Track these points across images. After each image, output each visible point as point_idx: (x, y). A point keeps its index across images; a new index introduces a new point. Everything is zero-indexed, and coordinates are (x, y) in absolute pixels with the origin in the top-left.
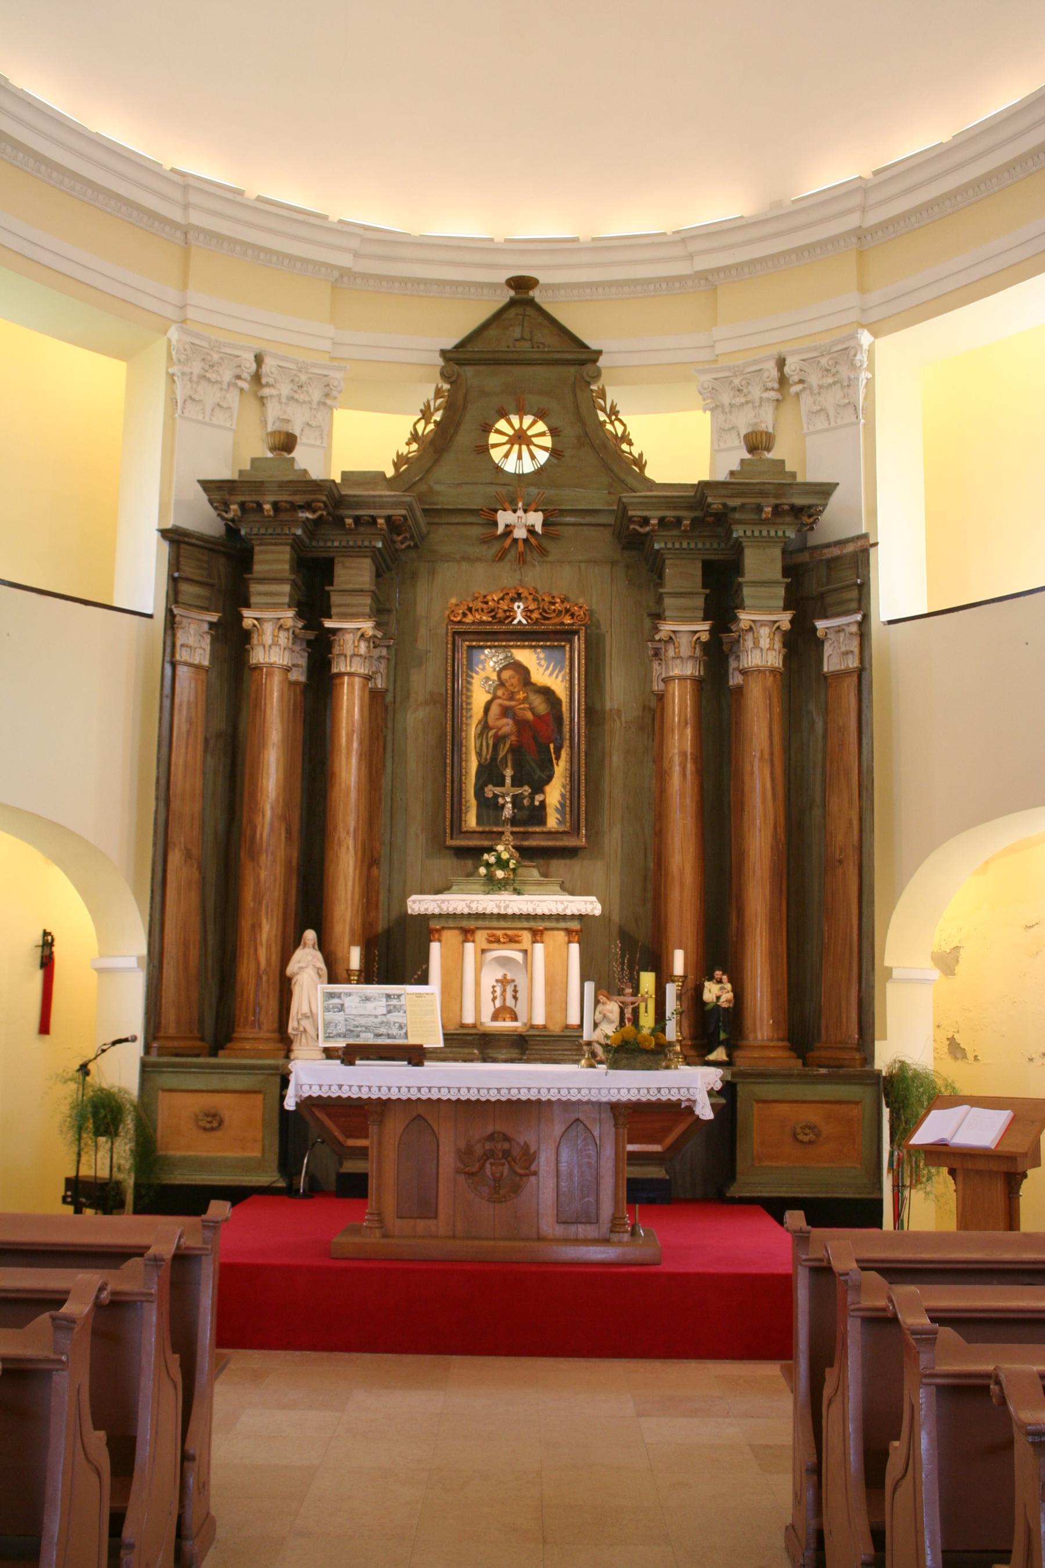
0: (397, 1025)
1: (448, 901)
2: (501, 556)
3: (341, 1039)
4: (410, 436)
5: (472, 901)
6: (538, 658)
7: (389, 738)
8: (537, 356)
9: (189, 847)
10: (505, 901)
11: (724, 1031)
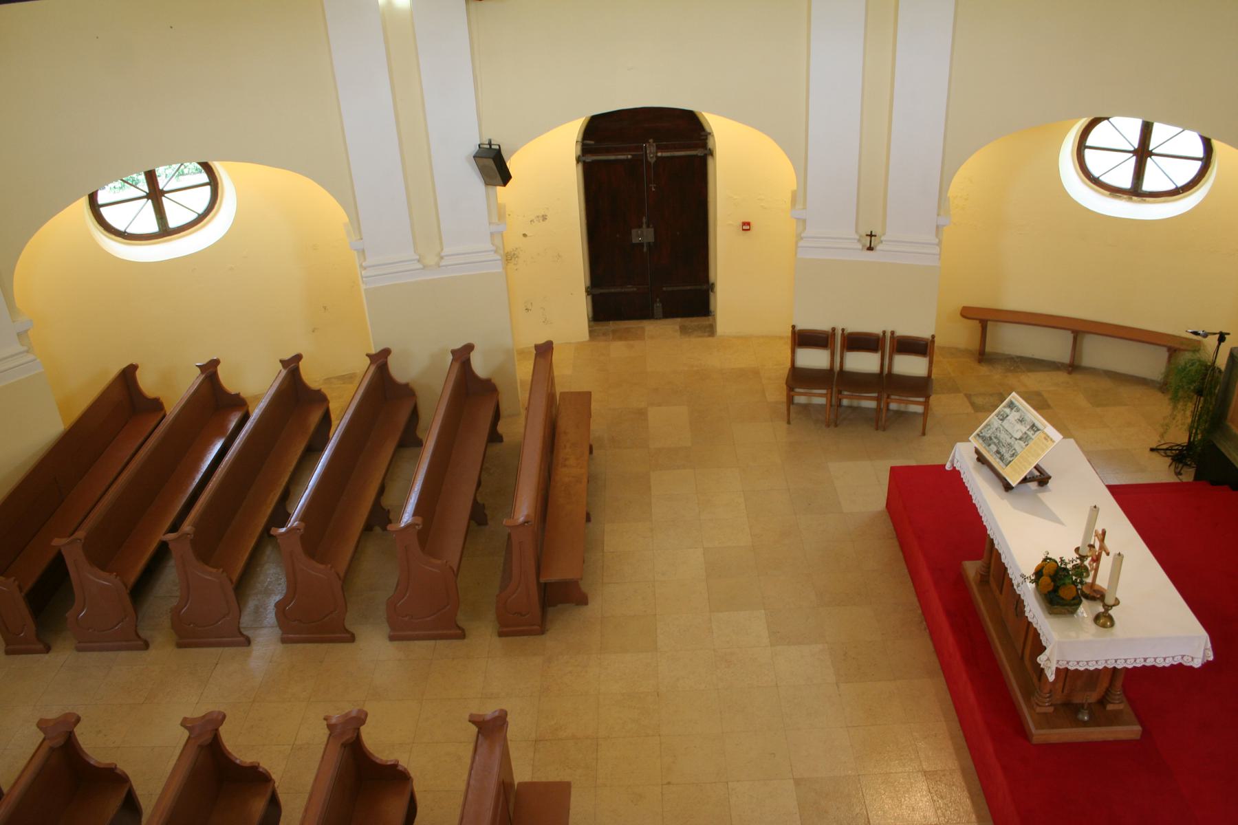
0: (1014, 451)
3: (981, 441)
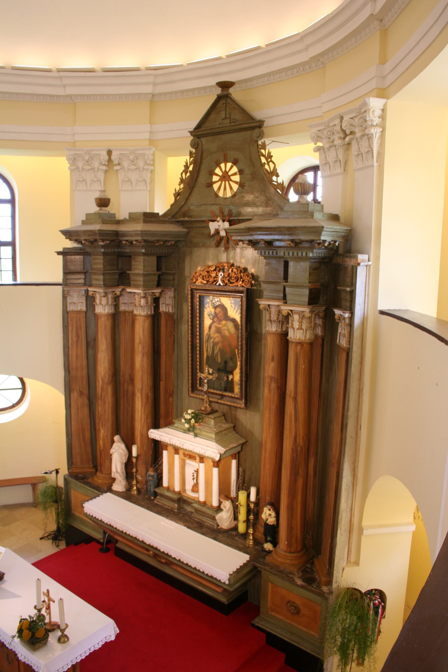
1: (163, 436)
2: (218, 245)
4: (180, 180)
5: (171, 438)
6: (231, 303)
7: (176, 336)
8: (233, 128)
9: (81, 390)
10: (182, 442)
11: (270, 536)
